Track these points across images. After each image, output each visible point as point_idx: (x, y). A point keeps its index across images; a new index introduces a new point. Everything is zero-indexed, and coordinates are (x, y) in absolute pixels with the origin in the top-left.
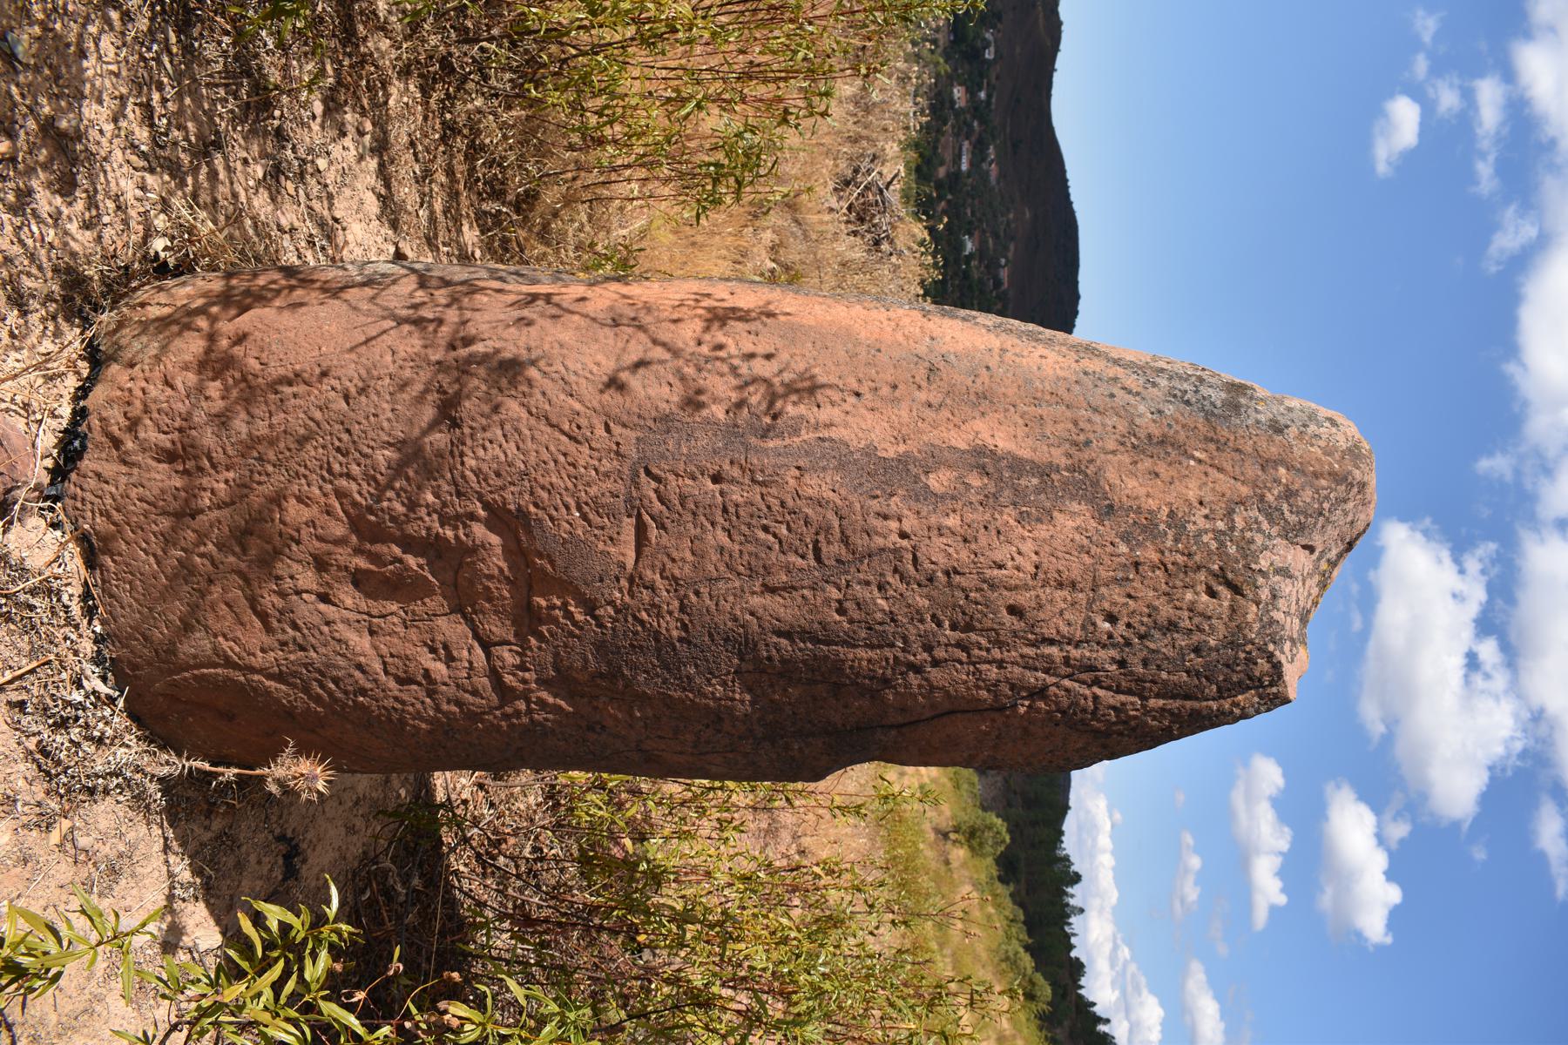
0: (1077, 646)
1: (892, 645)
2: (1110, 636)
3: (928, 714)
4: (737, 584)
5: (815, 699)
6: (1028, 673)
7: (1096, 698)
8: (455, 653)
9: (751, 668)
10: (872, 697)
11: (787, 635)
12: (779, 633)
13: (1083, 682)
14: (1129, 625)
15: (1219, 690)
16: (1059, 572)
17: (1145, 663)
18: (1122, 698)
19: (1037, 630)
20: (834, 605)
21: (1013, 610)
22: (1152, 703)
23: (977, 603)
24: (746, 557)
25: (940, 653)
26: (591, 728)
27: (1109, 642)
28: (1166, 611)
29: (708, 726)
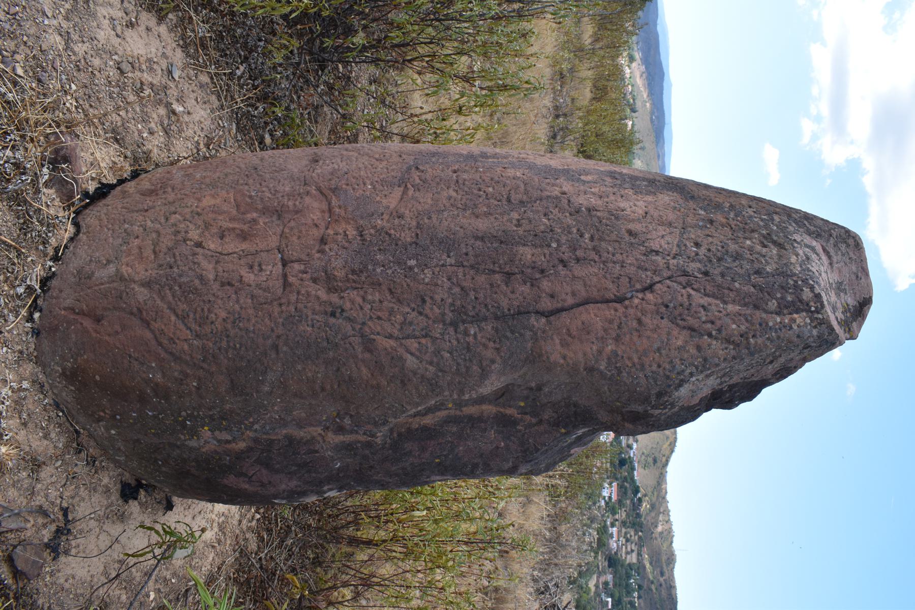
0: (674, 258)
1: (549, 246)
2: (697, 254)
3: (570, 301)
4: (456, 213)
5: (492, 285)
6: (640, 272)
7: (689, 296)
8: (264, 267)
9: (453, 262)
10: (532, 285)
11: (482, 239)
12: (476, 238)
13: (680, 283)
14: (709, 250)
15: (779, 306)
16: (660, 216)
17: (723, 275)
18: (710, 300)
19: (646, 244)
20: (515, 222)
21: (630, 233)
22: (730, 307)
23: (607, 225)
24: (464, 200)
25: (579, 253)
26: (333, 314)
27: (695, 258)
28: (733, 247)
29: (413, 310)
